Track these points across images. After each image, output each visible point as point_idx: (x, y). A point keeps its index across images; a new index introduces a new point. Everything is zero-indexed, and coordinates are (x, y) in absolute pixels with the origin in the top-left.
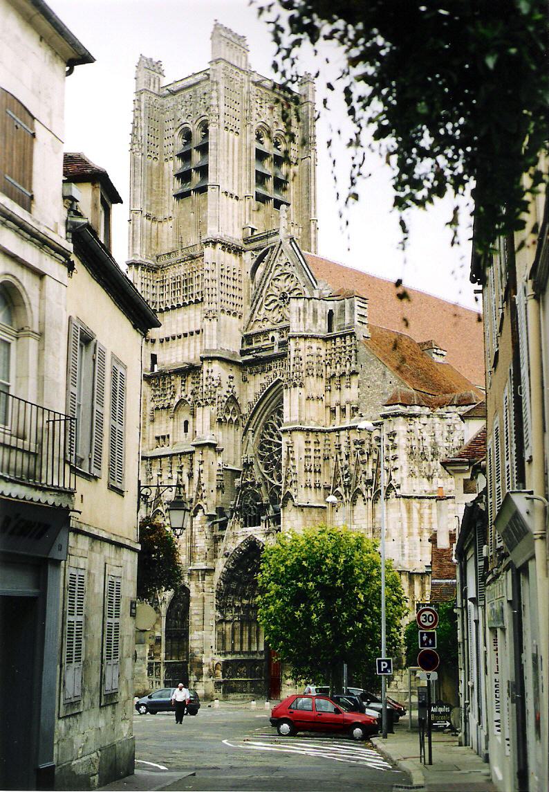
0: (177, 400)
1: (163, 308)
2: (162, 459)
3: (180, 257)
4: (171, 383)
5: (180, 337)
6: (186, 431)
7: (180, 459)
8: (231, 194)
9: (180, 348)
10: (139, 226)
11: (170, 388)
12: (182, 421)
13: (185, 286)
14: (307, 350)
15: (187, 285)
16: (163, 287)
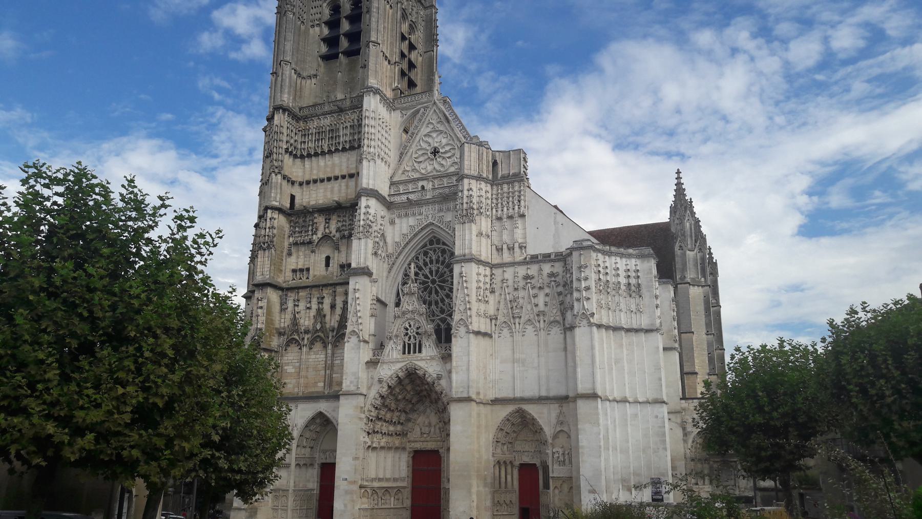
0: (320, 235)
1: (305, 154)
2: (300, 291)
3: (327, 108)
4: (313, 221)
5: (322, 181)
6: (327, 265)
7: (322, 290)
8: (386, 56)
9: (321, 191)
10: (288, 76)
11: (312, 225)
12: (324, 256)
13: (331, 135)
14: (478, 191)
15: (332, 134)
16: (305, 135)
